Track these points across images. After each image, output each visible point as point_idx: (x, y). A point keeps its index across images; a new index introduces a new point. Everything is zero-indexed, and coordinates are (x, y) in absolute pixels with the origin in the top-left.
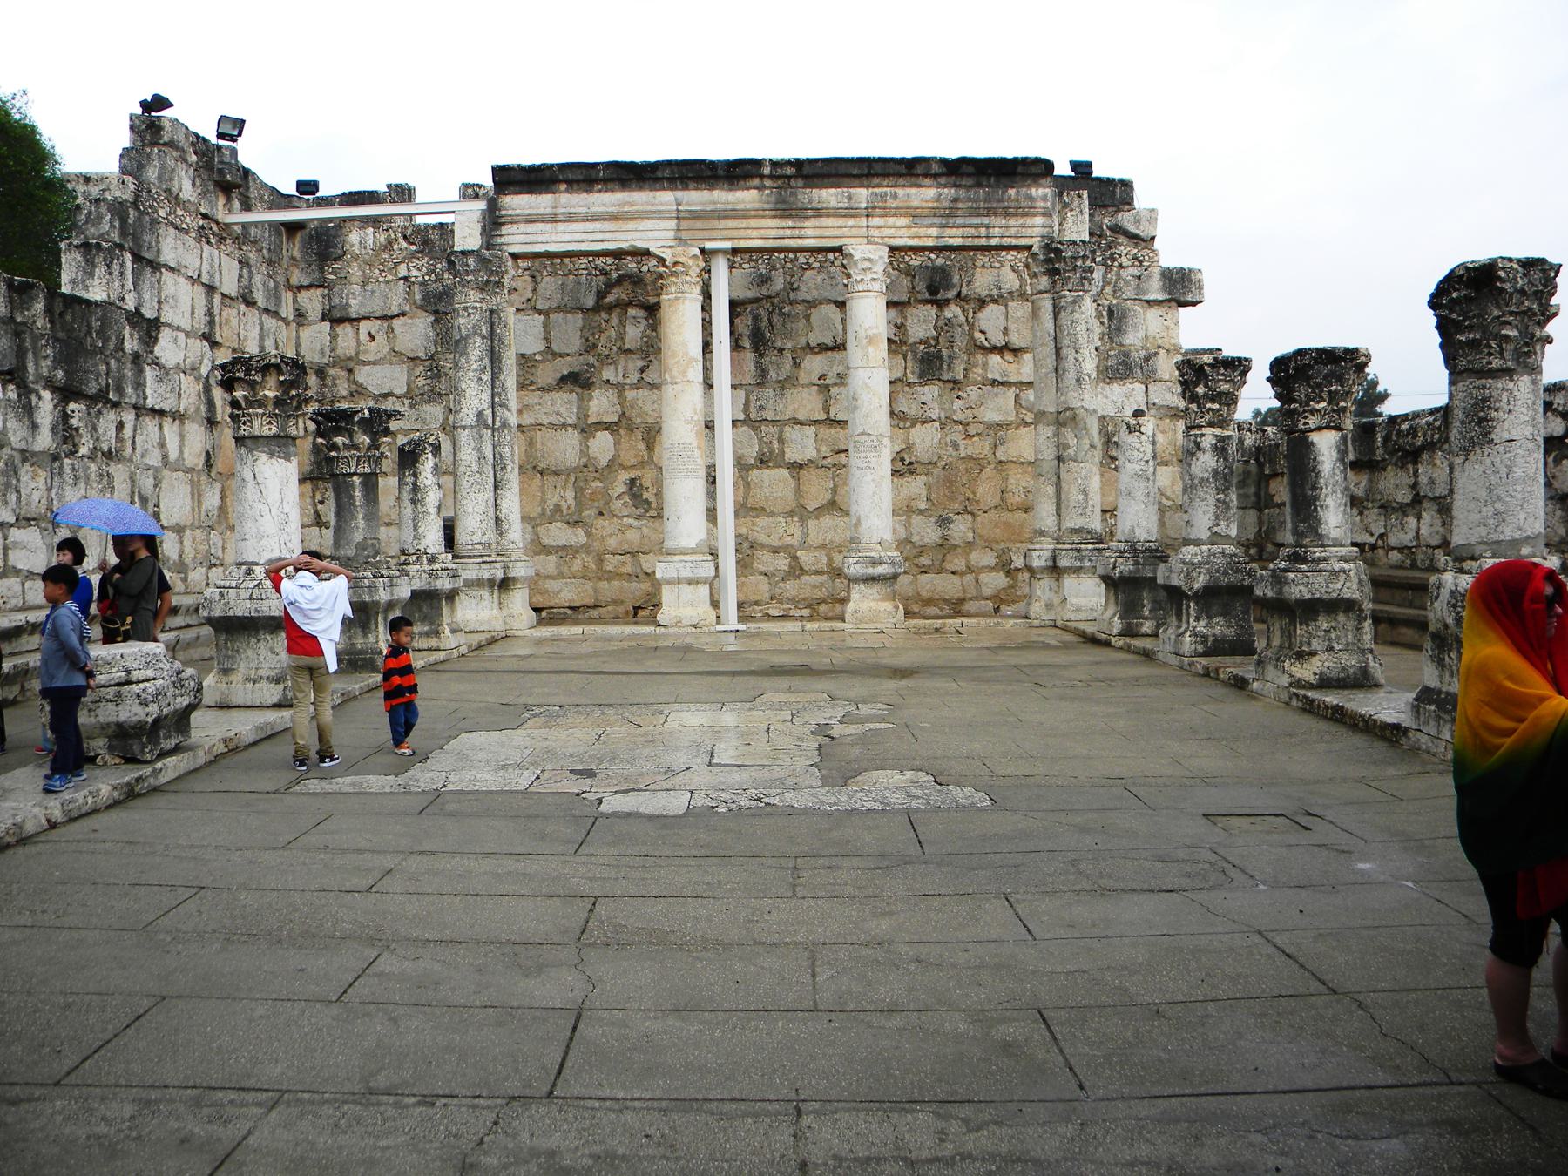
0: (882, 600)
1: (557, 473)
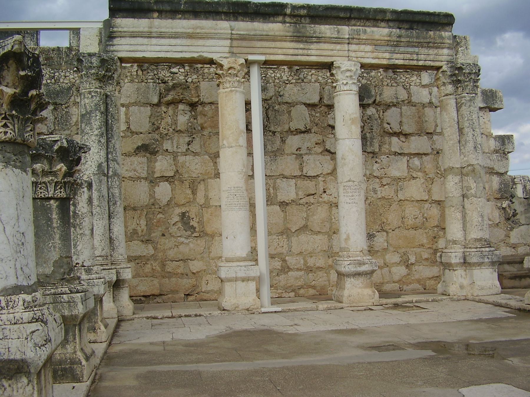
0: (366, 287)
1: (134, 209)
